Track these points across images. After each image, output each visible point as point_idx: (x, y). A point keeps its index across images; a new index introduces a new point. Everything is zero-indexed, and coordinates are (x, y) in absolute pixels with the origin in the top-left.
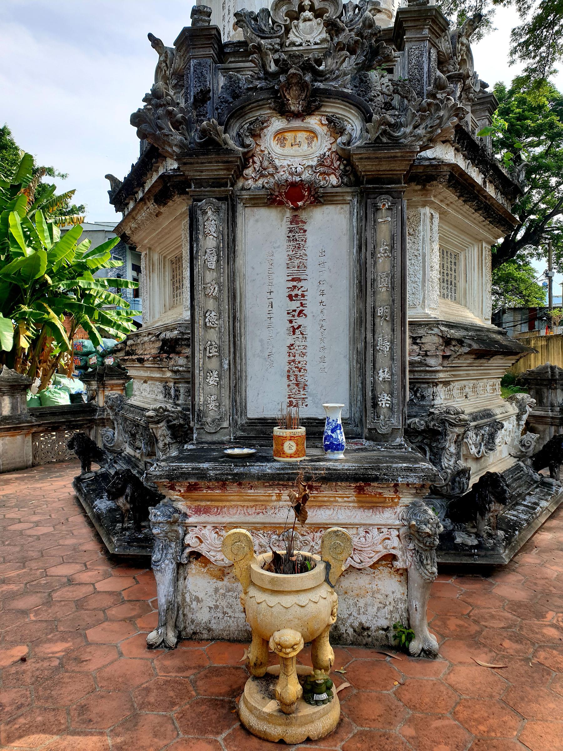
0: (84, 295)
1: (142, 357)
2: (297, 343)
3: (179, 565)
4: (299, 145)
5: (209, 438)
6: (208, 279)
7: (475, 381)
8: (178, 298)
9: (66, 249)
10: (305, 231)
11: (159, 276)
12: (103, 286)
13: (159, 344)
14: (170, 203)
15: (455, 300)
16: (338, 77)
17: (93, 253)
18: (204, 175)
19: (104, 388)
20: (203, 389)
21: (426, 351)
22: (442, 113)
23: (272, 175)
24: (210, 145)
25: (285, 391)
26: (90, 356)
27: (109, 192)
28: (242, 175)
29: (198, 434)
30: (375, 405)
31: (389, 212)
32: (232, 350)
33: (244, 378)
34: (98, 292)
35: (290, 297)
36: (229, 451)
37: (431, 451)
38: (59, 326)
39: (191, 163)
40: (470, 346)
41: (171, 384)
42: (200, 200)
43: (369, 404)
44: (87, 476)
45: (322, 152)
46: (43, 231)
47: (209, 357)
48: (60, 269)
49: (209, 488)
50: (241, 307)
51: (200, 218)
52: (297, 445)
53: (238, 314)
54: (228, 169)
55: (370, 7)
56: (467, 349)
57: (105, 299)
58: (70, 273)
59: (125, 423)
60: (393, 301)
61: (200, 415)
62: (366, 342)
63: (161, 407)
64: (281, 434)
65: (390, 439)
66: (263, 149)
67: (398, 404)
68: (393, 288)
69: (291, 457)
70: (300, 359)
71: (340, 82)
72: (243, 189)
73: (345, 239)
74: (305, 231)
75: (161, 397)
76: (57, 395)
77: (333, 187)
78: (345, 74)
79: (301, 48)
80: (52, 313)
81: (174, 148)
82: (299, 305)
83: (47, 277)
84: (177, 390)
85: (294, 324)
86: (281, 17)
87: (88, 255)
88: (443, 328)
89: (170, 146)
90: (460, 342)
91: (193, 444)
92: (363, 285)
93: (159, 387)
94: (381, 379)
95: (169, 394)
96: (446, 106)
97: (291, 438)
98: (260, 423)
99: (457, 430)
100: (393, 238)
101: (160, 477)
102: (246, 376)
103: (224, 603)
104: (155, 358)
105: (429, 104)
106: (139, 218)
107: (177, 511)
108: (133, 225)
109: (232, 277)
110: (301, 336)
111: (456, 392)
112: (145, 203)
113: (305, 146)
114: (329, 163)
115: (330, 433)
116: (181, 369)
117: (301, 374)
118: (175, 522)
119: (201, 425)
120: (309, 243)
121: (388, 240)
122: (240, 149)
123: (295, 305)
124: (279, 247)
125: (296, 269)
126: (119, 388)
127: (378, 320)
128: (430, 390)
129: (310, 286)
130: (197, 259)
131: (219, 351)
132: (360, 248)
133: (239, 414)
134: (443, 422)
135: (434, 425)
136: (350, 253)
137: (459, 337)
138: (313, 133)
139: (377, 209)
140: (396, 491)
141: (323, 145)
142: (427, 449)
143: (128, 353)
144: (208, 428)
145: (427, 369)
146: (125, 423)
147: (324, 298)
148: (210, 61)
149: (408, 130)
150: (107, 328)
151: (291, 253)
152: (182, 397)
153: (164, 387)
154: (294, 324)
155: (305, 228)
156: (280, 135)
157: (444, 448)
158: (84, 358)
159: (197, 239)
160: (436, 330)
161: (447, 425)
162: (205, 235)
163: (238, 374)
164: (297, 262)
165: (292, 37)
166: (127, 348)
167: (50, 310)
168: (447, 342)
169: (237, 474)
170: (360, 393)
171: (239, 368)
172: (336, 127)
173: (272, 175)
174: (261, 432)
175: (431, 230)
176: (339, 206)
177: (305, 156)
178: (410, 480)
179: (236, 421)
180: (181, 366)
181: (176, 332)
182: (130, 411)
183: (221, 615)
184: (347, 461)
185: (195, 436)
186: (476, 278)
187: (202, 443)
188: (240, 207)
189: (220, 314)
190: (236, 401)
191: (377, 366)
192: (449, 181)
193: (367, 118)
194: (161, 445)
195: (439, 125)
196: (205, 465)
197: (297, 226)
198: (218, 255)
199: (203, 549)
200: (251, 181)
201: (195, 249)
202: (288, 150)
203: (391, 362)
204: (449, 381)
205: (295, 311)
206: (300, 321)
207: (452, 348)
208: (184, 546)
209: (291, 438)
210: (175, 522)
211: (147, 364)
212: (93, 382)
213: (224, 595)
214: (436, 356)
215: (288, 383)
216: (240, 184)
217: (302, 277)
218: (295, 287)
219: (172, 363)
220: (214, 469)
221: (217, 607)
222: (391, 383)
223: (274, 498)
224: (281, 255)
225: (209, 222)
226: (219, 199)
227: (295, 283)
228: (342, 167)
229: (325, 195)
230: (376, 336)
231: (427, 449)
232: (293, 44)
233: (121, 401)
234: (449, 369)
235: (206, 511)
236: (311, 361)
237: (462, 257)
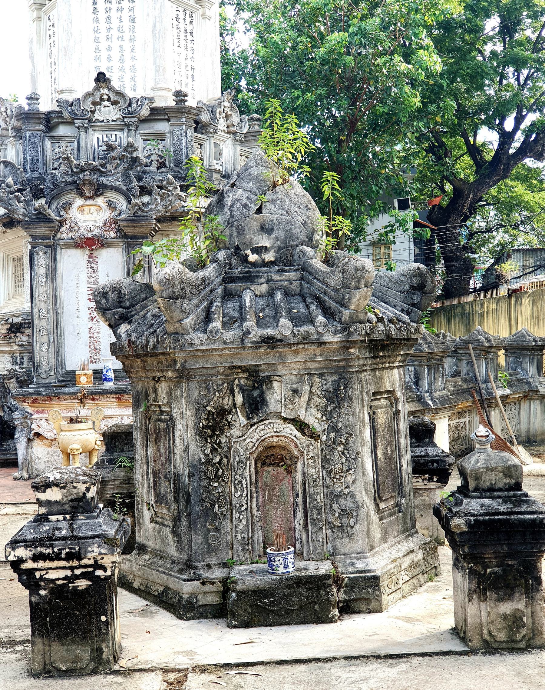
2: (95, 326)
3: (29, 440)
4: (92, 214)
5: (43, 381)
18: (37, 234)
22: (171, 198)
25: (88, 355)
32: (55, 331)
41: (18, 355)
42: (35, 248)
53: (59, 310)
55: (147, 102)
61: (37, 369)
71: (115, 178)
72: (60, 239)
78: (118, 173)
79: (103, 124)
81: (20, 216)
84: (22, 359)
86: (88, 106)
89: (17, 214)
93: (8, 357)
95: (16, 362)
97: (85, 375)
101: (18, 395)
103: (51, 459)
105: (164, 193)
107: (27, 412)
116: (24, 343)
118: (26, 417)
120: (100, 269)
122: (58, 218)
131: (48, 332)
141: (106, 214)
144: (42, 376)
148: (40, 133)
149: (153, 207)
152: (25, 363)
153: (12, 357)
156: (81, 208)
159: (34, 269)
162: (39, 267)
164: (93, 280)
165: (97, 116)
172: (111, 206)
181: (20, 319)
183: (50, 466)
188: (59, 249)
197: (92, 260)
198: (46, 278)
199: (40, 431)
200: (64, 234)
202: (86, 217)
208: (31, 430)
209: (85, 375)
210: (26, 417)
213: (52, 455)
216: (58, 236)
219: (18, 339)
221: (48, 461)
226: (46, 247)
232: (99, 121)
235: (42, 412)
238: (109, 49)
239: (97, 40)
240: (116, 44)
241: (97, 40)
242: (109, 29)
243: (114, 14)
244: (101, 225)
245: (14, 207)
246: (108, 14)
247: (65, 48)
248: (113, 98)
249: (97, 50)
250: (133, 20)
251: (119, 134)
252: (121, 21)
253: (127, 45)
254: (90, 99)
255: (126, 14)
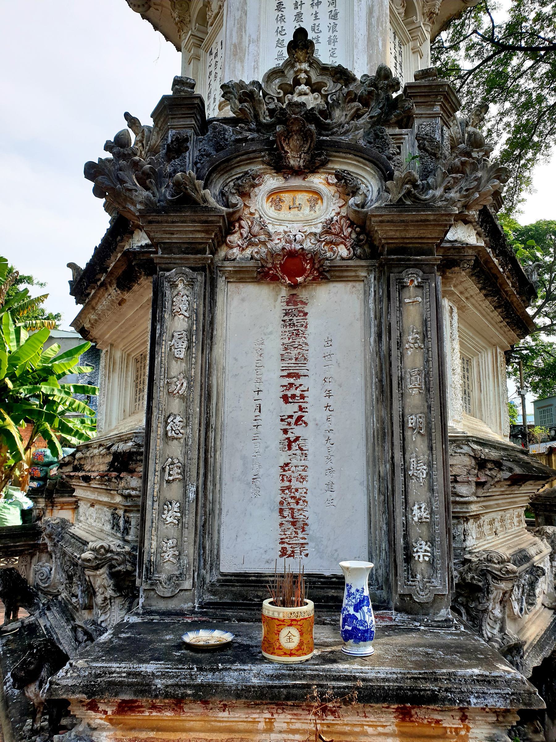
0: (47, 400)
1: (89, 474)
2: (294, 462)
4: (299, 208)
5: (162, 605)
6: (173, 373)
7: (502, 513)
8: (141, 402)
9: (31, 352)
10: (306, 314)
11: (120, 377)
12: (68, 393)
13: (109, 459)
14: (136, 287)
15: (470, 412)
16: (347, 131)
17: (60, 357)
18: (176, 238)
19: (53, 506)
20: (157, 529)
21: (455, 476)
22: (479, 174)
23: (264, 243)
24: (185, 201)
25: (277, 534)
26: (51, 467)
27: (70, 282)
28: (225, 242)
29: (147, 598)
30: (409, 558)
31: (419, 291)
32: (202, 471)
33: (217, 512)
34: (62, 399)
35: (285, 398)
36: (190, 637)
37: (468, 613)
38: (14, 434)
39: (158, 222)
40: (511, 470)
41: (121, 512)
42: (169, 270)
43: (401, 556)
44: (10, 627)
45: (328, 217)
46: (9, 334)
47: (168, 482)
48: (23, 373)
49: (154, 707)
50: (217, 410)
51: (168, 292)
52: (301, 634)
53: (213, 420)
54: (207, 232)
56: (508, 475)
57: (69, 406)
58: (34, 378)
59: (64, 558)
60: (429, 407)
61: (151, 570)
62: (393, 465)
63: (102, 547)
64: (276, 615)
65: (431, 611)
66: (252, 210)
67: (442, 557)
68: (428, 390)
69: (291, 655)
70: (298, 485)
72: (226, 259)
73: (358, 327)
74: (306, 314)
75: (108, 527)
76: (6, 511)
77: (343, 259)
80: (8, 419)
82: (297, 409)
83: (7, 380)
84: (127, 522)
85: (289, 435)
87: (55, 360)
88: (475, 447)
90: (498, 464)
91: (137, 614)
92: (385, 385)
93: (107, 514)
94: (416, 519)
95: (118, 525)
96: (485, 166)
97: (292, 623)
98: (238, 581)
99: (503, 585)
100: (425, 323)
101: (72, 689)
102: (220, 509)
104: (102, 476)
105: (463, 163)
106: (99, 307)
108: (93, 317)
109: (207, 370)
110: (299, 452)
111: (486, 528)
112: (107, 289)
113: (306, 210)
114: (338, 230)
115: (352, 611)
116: (133, 493)
117: (299, 507)
119: (152, 584)
121: (419, 327)
122: (224, 208)
123: (291, 409)
124: (271, 333)
125: (293, 361)
126: (70, 507)
127: (408, 433)
128: (461, 528)
129: (312, 385)
130: (160, 344)
131: (183, 473)
132: (379, 336)
133: (208, 567)
134: (484, 573)
135: (473, 578)
136: (366, 343)
137: (496, 458)
138: (317, 195)
139: (403, 287)
140: (464, 718)
141: (330, 208)
142: (463, 611)
143: (76, 469)
144: (161, 590)
145: (458, 499)
146: (64, 558)
147: (330, 401)
149: (438, 192)
150: (68, 437)
151: (286, 341)
153: (113, 514)
154: (289, 435)
155: (306, 310)
156: (274, 196)
157: (485, 611)
158: (45, 468)
159: (162, 318)
161: (489, 577)
162: (173, 315)
163: (209, 506)
164: (294, 352)
166: (76, 462)
167: (6, 416)
168: (481, 464)
169: (201, 685)
170: (385, 538)
171: (210, 497)
172: (347, 186)
173: (264, 243)
174: (240, 597)
175: (452, 326)
176: (350, 284)
177: (307, 222)
178: (491, 702)
179: (204, 579)
180: (133, 489)
181: (130, 444)
182: (70, 543)
184: (379, 660)
185: (141, 601)
186: (491, 388)
187: (150, 613)
188: (221, 282)
189: (188, 419)
190: (204, 548)
191: (411, 499)
192: (474, 267)
193: (386, 175)
194: (99, 599)
195: (477, 188)
196: (149, 668)
198: (190, 341)
200: (237, 250)
201: (158, 332)
202: (285, 214)
203: (429, 494)
204: (479, 514)
205: (291, 417)
206: (298, 431)
207: (488, 473)
209: (292, 623)
211: (94, 484)
212: (40, 500)
214: (468, 482)
215: (280, 521)
216: (222, 252)
217: (301, 372)
218: (291, 385)
219: (122, 484)
220: (164, 675)
222: (430, 525)
223: (261, 726)
224: (274, 344)
225: (179, 298)
226: (194, 269)
227: (292, 380)
228: (354, 236)
229: (332, 269)
230: (407, 456)
231: (463, 611)
233: (63, 528)
234: (482, 499)
236: (313, 487)
237: (474, 363)
244: (318, 230)
245: (129, 185)
246: (298, 10)
247: (235, 46)
248: (314, 78)
250: (334, 16)
252: (316, 18)
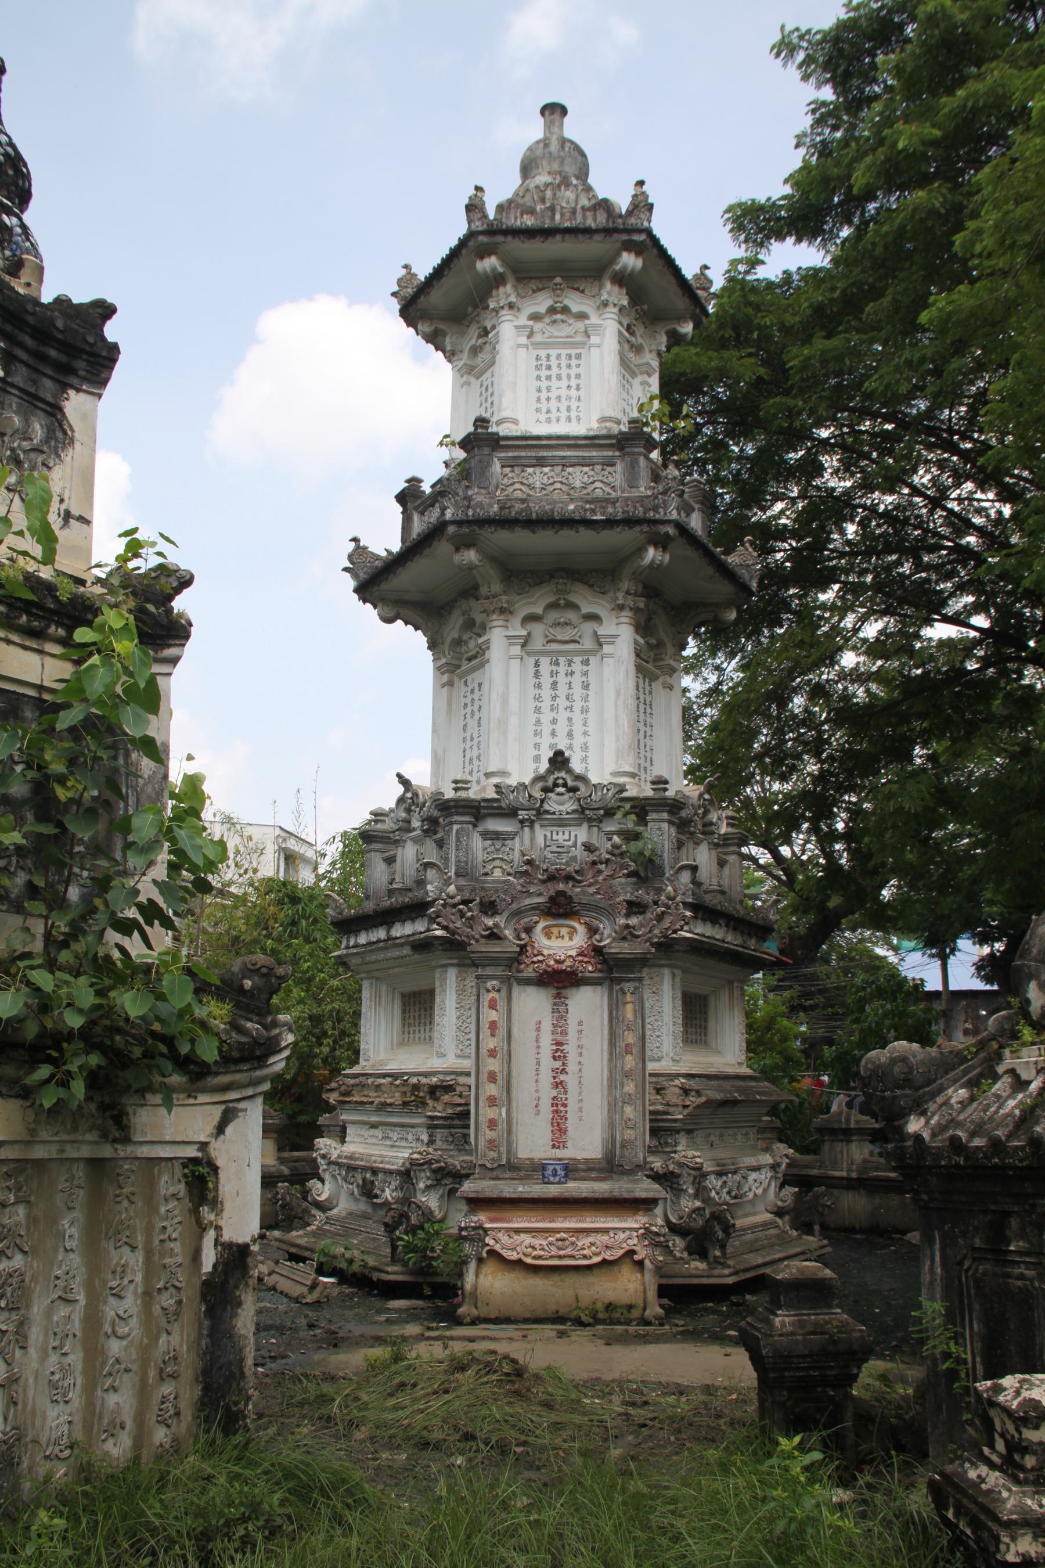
25: (550, 1135)
35: (554, 1058)
123: (558, 1064)
129: (571, 1049)
160: (677, 1082)
165: (546, 807)
202: (554, 943)
206: (562, 1077)
238: (554, 721)
239: (538, 710)
240: (563, 716)
241: (538, 710)
242: (554, 698)
243: (562, 679)
248: (570, 783)
249: (538, 722)
250: (586, 687)
251: (574, 831)
252: (570, 688)
253: (577, 717)
254: (540, 785)
255: (577, 680)
